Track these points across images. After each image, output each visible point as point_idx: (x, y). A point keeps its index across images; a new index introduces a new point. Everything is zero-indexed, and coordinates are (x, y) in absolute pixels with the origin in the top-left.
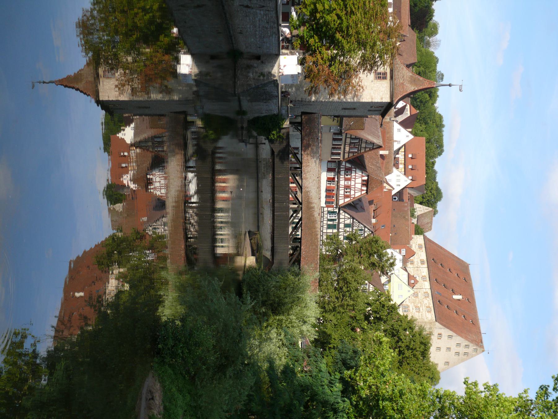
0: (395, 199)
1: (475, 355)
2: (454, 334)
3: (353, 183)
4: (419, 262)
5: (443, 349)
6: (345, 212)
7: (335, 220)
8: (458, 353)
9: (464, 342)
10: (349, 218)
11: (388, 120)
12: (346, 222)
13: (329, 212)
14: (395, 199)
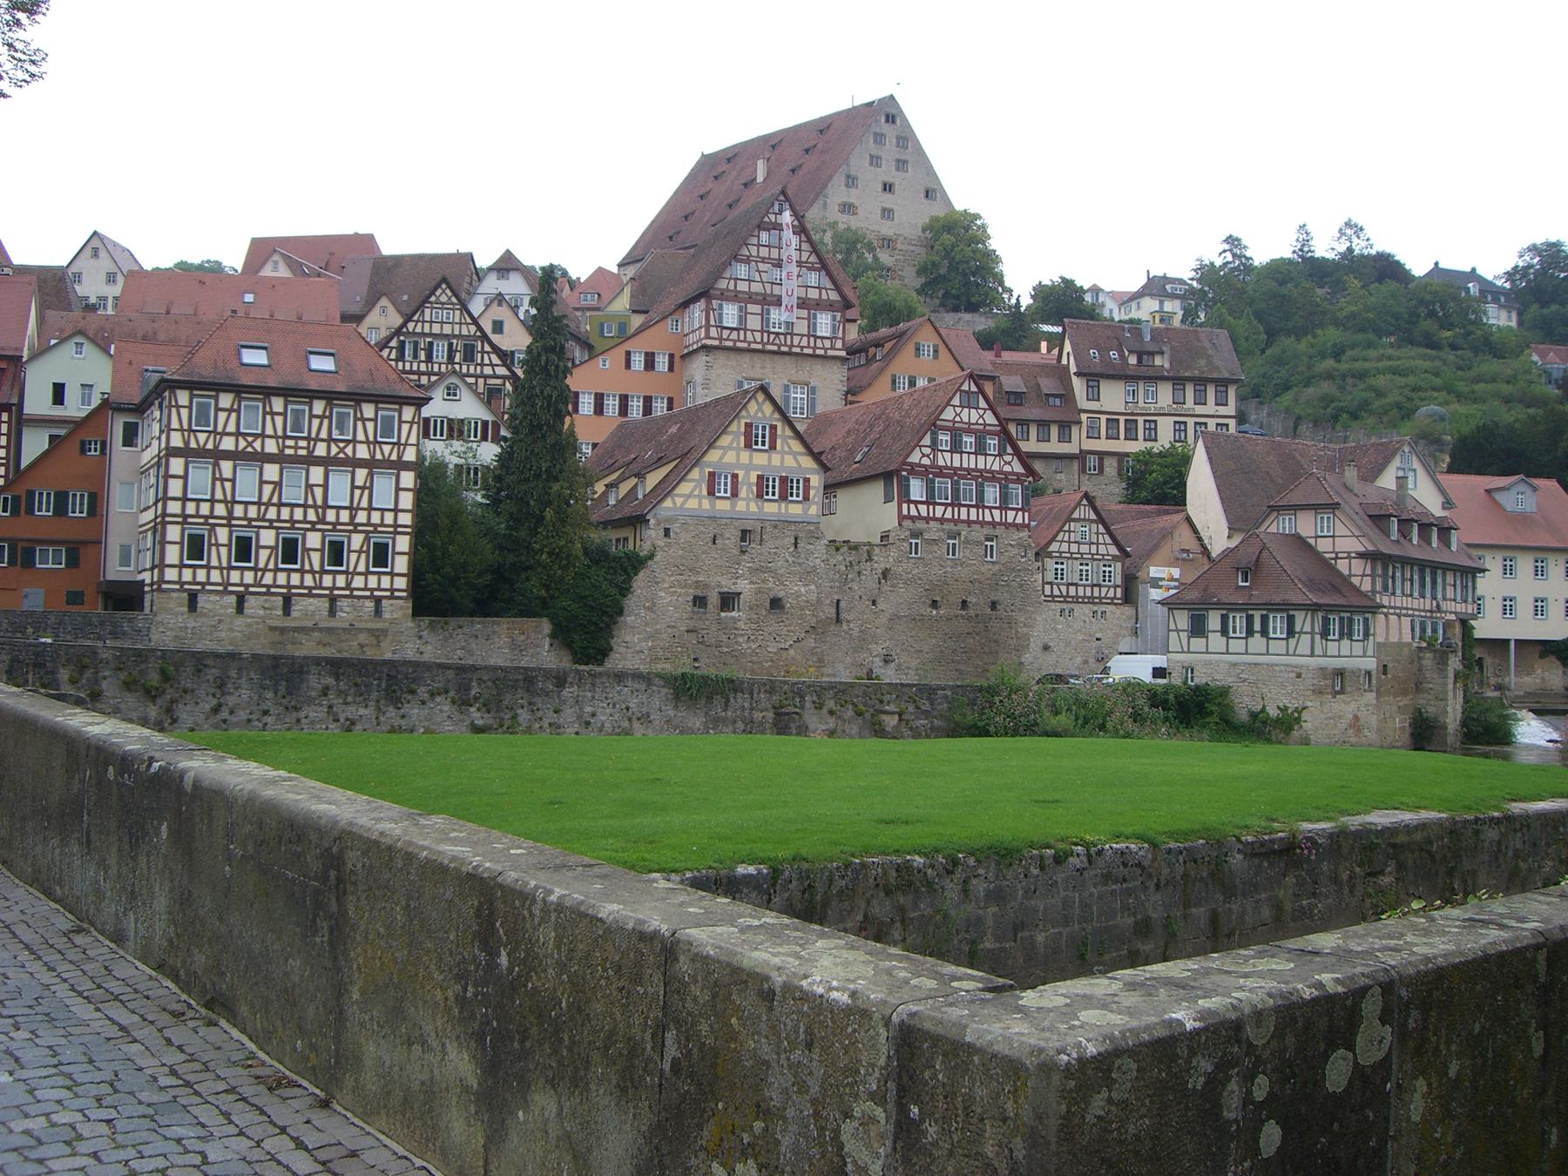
2: (843, 170)
5: (888, 200)
8: (901, 164)
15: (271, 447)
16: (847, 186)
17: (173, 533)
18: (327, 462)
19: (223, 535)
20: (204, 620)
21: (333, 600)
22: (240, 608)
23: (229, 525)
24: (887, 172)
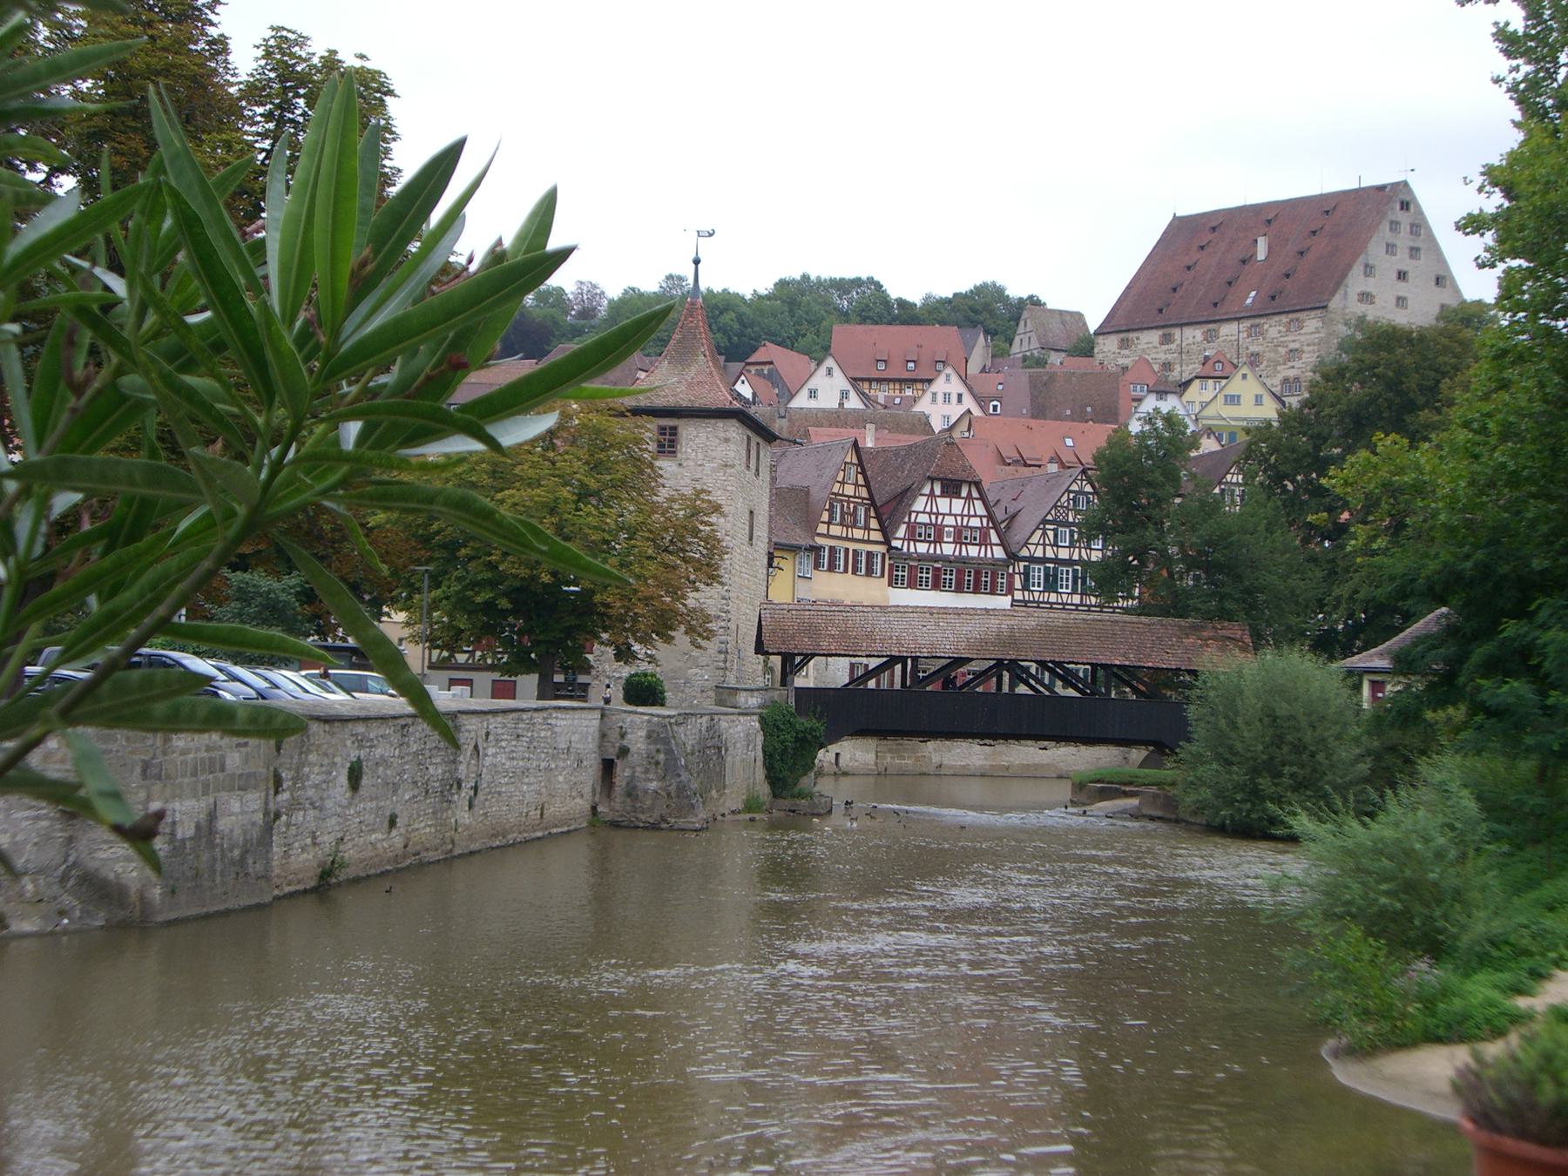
0: (995, 407)
1: (1418, 206)
2: (1361, 260)
3: (950, 521)
4: (1165, 347)
5: (1402, 289)
6: (1026, 544)
7: (1047, 569)
8: (1414, 252)
9: (1384, 233)
10: (1044, 534)
11: (784, 423)
13: (1025, 588)
14: (995, 407)
16: (1366, 275)
24: (1402, 260)
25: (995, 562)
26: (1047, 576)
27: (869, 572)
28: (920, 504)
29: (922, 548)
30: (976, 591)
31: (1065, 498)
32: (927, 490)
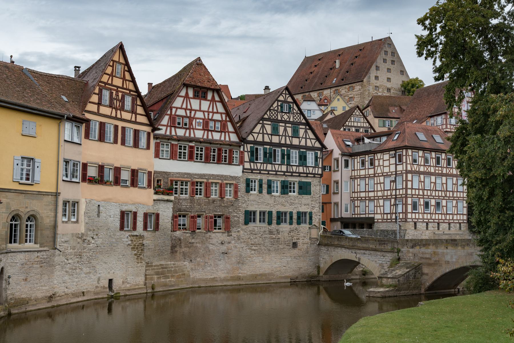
3: (199, 115)
6: (251, 132)
10: (263, 127)
12: (269, 132)
13: (251, 161)
15: (433, 171)
17: (409, 201)
18: (446, 175)
19: (422, 200)
20: (419, 232)
21: (449, 224)
22: (427, 228)
23: (423, 198)
25: (231, 144)
26: (265, 153)
27: (136, 145)
28: (178, 102)
29: (181, 132)
30: (219, 162)
31: (275, 105)
32: (183, 93)
